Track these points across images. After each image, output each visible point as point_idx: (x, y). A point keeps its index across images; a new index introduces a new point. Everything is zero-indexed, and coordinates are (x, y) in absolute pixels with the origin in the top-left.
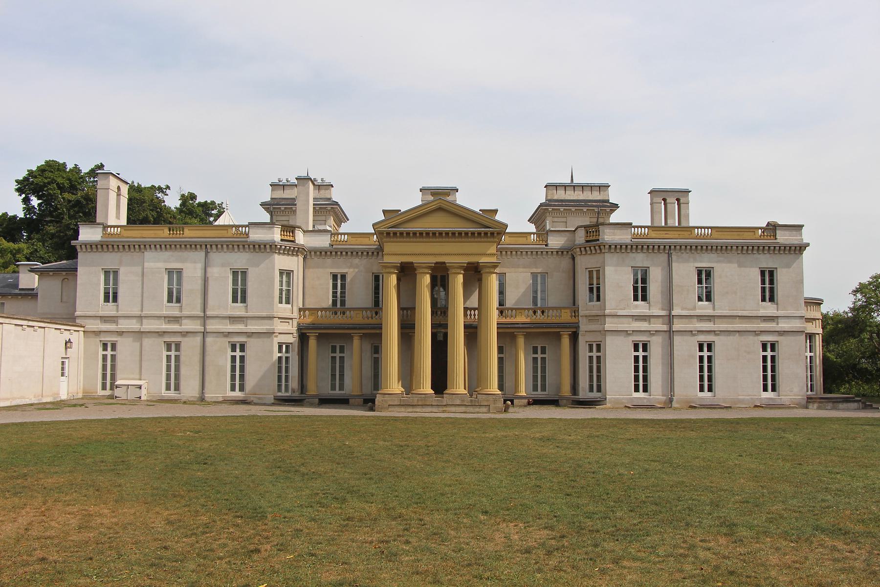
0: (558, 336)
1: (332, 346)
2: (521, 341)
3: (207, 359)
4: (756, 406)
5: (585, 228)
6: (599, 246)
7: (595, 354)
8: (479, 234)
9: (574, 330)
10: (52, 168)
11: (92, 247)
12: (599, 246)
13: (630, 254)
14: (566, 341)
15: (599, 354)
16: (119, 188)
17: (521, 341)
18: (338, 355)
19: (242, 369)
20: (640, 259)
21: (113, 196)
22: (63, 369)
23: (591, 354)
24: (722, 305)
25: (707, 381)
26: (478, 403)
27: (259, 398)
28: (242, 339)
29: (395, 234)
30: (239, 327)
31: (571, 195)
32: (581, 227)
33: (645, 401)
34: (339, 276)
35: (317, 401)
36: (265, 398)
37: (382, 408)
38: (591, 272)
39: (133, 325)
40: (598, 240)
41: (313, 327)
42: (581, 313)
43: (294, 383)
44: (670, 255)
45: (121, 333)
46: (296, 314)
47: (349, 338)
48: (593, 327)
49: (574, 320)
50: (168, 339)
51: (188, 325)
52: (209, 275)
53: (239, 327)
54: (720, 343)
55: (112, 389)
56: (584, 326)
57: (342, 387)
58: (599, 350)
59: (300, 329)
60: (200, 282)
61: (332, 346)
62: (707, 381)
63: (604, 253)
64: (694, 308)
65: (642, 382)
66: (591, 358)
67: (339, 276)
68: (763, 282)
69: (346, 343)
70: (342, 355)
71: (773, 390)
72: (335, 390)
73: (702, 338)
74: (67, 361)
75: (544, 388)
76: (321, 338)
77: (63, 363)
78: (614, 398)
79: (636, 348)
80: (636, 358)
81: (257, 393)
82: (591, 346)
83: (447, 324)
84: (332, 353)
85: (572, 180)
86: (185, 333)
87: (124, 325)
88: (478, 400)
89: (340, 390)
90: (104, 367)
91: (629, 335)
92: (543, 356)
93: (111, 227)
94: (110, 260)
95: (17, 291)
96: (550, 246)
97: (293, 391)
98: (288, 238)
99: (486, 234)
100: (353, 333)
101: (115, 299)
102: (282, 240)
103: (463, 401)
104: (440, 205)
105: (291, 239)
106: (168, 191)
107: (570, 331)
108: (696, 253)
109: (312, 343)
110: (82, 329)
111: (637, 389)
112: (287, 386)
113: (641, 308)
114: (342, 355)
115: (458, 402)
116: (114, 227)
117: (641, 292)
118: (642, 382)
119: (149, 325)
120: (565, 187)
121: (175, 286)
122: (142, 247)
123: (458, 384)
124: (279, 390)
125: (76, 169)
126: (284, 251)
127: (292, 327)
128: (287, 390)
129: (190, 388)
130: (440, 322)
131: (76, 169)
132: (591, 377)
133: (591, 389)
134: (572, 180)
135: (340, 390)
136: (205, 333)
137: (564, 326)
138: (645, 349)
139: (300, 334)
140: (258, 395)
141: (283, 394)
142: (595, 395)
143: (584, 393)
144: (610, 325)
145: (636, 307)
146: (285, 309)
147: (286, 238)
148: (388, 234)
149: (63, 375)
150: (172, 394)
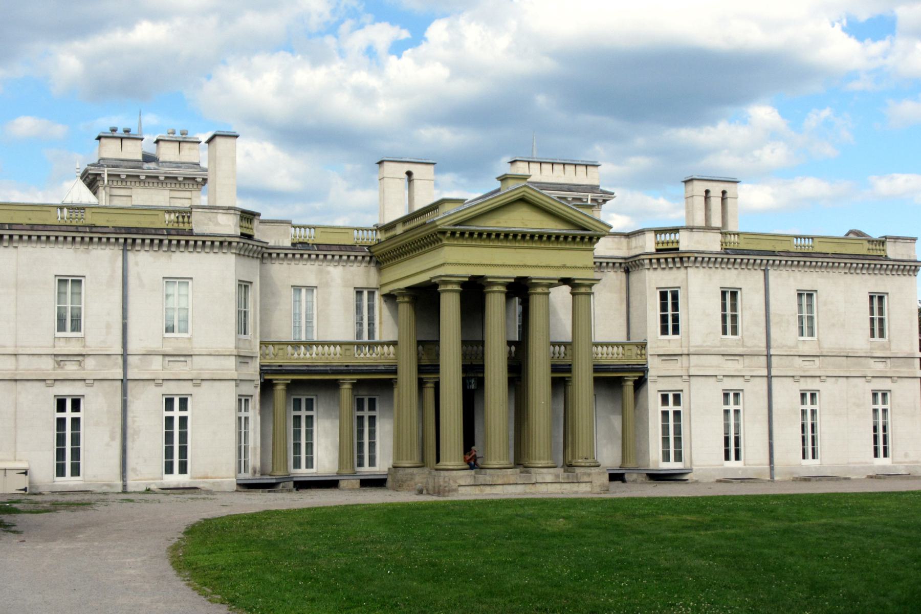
1: (295, 400)
4: (871, 477)
5: (655, 231)
6: (681, 258)
7: (671, 408)
8: (574, 238)
9: (641, 374)
12: (681, 258)
18: (303, 413)
19: (183, 437)
20: (730, 277)
23: (665, 408)
26: (577, 480)
29: (462, 234)
32: (649, 230)
33: (740, 472)
35: (291, 484)
36: (222, 482)
37: (449, 491)
38: (663, 295)
40: (677, 249)
41: (281, 371)
42: (650, 350)
44: (766, 272)
46: (257, 349)
47: (334, 386)
53: (180, 369)
56: (655, 367)
57: (310, 463)
61: (295, 400)
63: (686, 267)
66: (665, 414)
68: (872, 313)
69: (316, 395)
70: (310, 413)
71: (885, 455)
72: (300, 467)
76: (292, 387)
78: (702, 469)
81: (209, 475)
82: (665, 399)
83: (439, 365)
84: (166, 410)
86: (161, 382)
88: (577, 474)
89: (307, 467)
91: (720, 381)
99: (582, 238)
100: (344, 379)
101: (76, 327)
103: (557, 476)
104: (524, 195)
107: (635, 376)
108: (790, 270)
111: (727, 457)
114: (310, 413)
119: (27, 366)
126: (254, 254)
127: (253, 371)
130: (471, 362)
132: (666, 440)
133: (666, 457)
135: (307, 467)
136: (124, 380)
139: (262, 381)
140: (211, 478)
142: (672, 465)
148: (453, 234)
150: (176, 479)
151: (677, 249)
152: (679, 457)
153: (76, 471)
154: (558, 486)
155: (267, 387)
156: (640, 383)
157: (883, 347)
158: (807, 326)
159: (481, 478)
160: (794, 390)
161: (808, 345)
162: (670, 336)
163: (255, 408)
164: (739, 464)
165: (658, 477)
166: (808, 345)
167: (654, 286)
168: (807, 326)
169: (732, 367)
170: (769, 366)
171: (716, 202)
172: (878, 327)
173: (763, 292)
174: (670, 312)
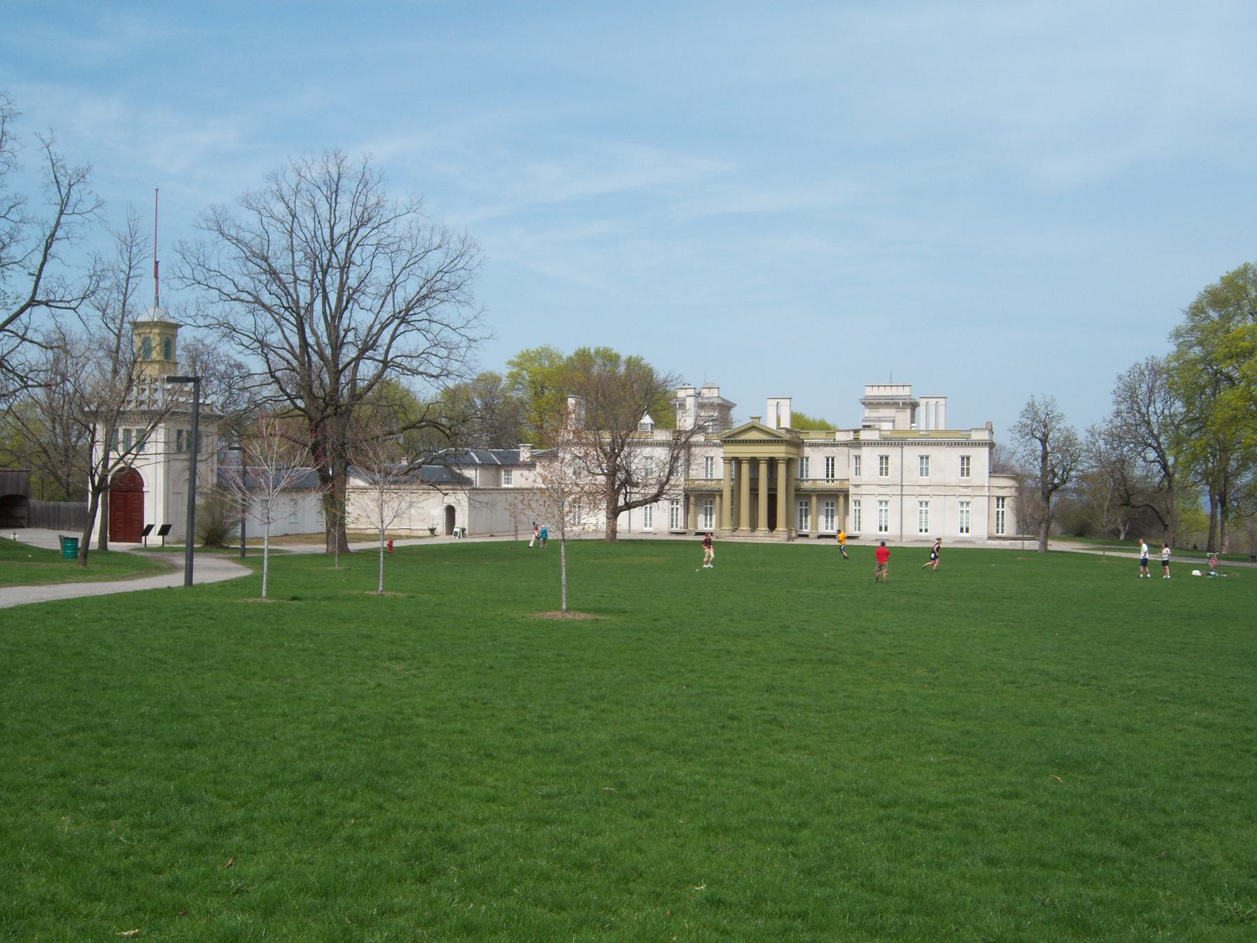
2: (814, 499)
8: (775, 441)
14: (841, 500)
17: (814, 499)
20: (884, 451)
24: (933, 477)
41: (693, 490)
42: (851, 482)
43: (681, 523)
47: (715, 497)
54: (932, 501)
56: (852, 490)
58: (859, 505)
109: (692, 499)
117: (884, 471)
124: (672, 526)
128: (677, 527)
137: (840, 491)
141: (674, 529)
142: (856, 533)
144: (863, 490)
155: (687, 498)
156: (846, 497)
157: (967, 481)
158: (924, 472)
159: (735, 533)
161: (924, 480)
162: (858, 476)
166: (924, 480)
168: (924, 472)
169: (883, 490)
171: (932, 408)
172: (965, 471)
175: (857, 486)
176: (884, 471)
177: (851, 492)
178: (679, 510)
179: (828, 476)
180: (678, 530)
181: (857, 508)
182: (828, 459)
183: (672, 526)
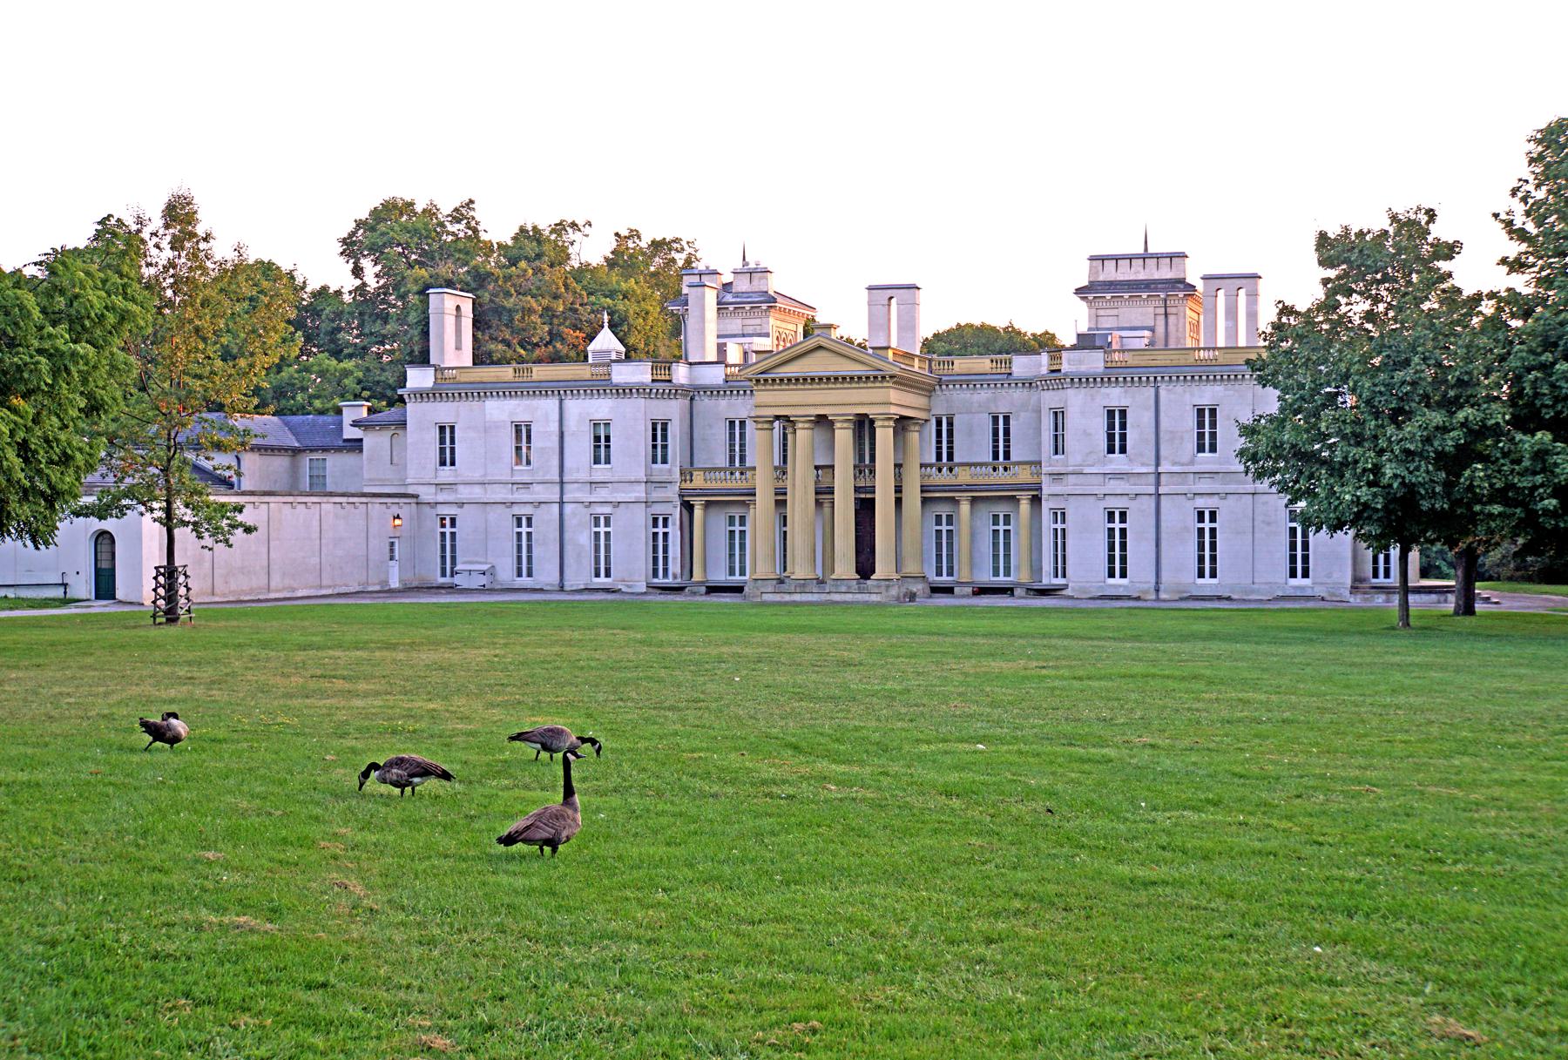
0: (1014, 500)
3: (567, 536)
10: (390, 210)
11: (422, 395)
13: (1103, 390)
14: (1025, 506)
15: (1123, 526)
16: (458, 308)
17: (965, 507)
20: (1115, 396)
21: (450, 321)
22: (392, 551)
25: (1207, 564)
27: (629, 586)
28: (607, 509)
30: (602, 494)
31: (1138, 273)
34: (737, 423)
35: (703, 589)
39: (477, 493)
40: (1059, 371)
42: (1044, 470)
43: (675, 567)
45: (461, 505)
46: (677, 475)
48: (1057, 489)
49: (1035, 480)
50: (517, 510)
51: (540, 493)
52: (565, 429)
54: (1225, 509)
55: (452, 576)
58: (1064, 521)
59: (681, 496)
60: (556, 439)
62: (1207, 564)
64: (1192, 463)
65: (1117, 564)
67: (737, 423)
73: (1201, 503)
74: (396, 541)
75: (1007, 573)
77: (392, 544)
79: (1111, 516)
80: (1201, 531)
85: (1146, 249)
87: (464, 493)
90: (443, 548)
92: (1007, 528)
93: (449, 368)
94: (444, 412)
95: (341, 443)
96: (1015, 375)
97: (675, 577)
98: (663, 378)
102: (653, 381)
103: (849, 587)
105: (667, 378)
106: (587, 230)
110: (414, 500)
112: (666, 571)
113: (1118, 462)
115: (843, 589)
116: (453, 368)
117: (1116, 442)
118: (1117, 564)
120: (1130, 258)
121: (524, 445)
122: (482, 391)
123: (883, 567)
124: (655, 574)
125: (430, 212)
127: (672, 492)
129: (546, 574)
131: (430, 212)
134: (1146, 249)
138: (1213, 518)
141: (660, 580)
142: (1060, 581)
143: (1048, 580)
145: (1111, 461)
146: (661, 470)
147: (659, 377)
149: (392, 558)
151: (1059, 371)
152: (1064, 576)
153: (530, 574)
154: (850, 596)
155: (688, 507)
156: (1036, 500)
160: (584, 515)
163: (674, 524)
164: (1124, 581)
165: (1044, 592)
167: (1047, 407)
170: (1158, 484)
173: (1153, 409)
174: (1060, 432)
175: (1057, 476)
176: (1116, 442)
177: (1046, 491)
178: (670, 536)
179: (996, 456)
180: (670, 581)
181: (1059, 526)
182: (995, 419)
183: (655, 574)
